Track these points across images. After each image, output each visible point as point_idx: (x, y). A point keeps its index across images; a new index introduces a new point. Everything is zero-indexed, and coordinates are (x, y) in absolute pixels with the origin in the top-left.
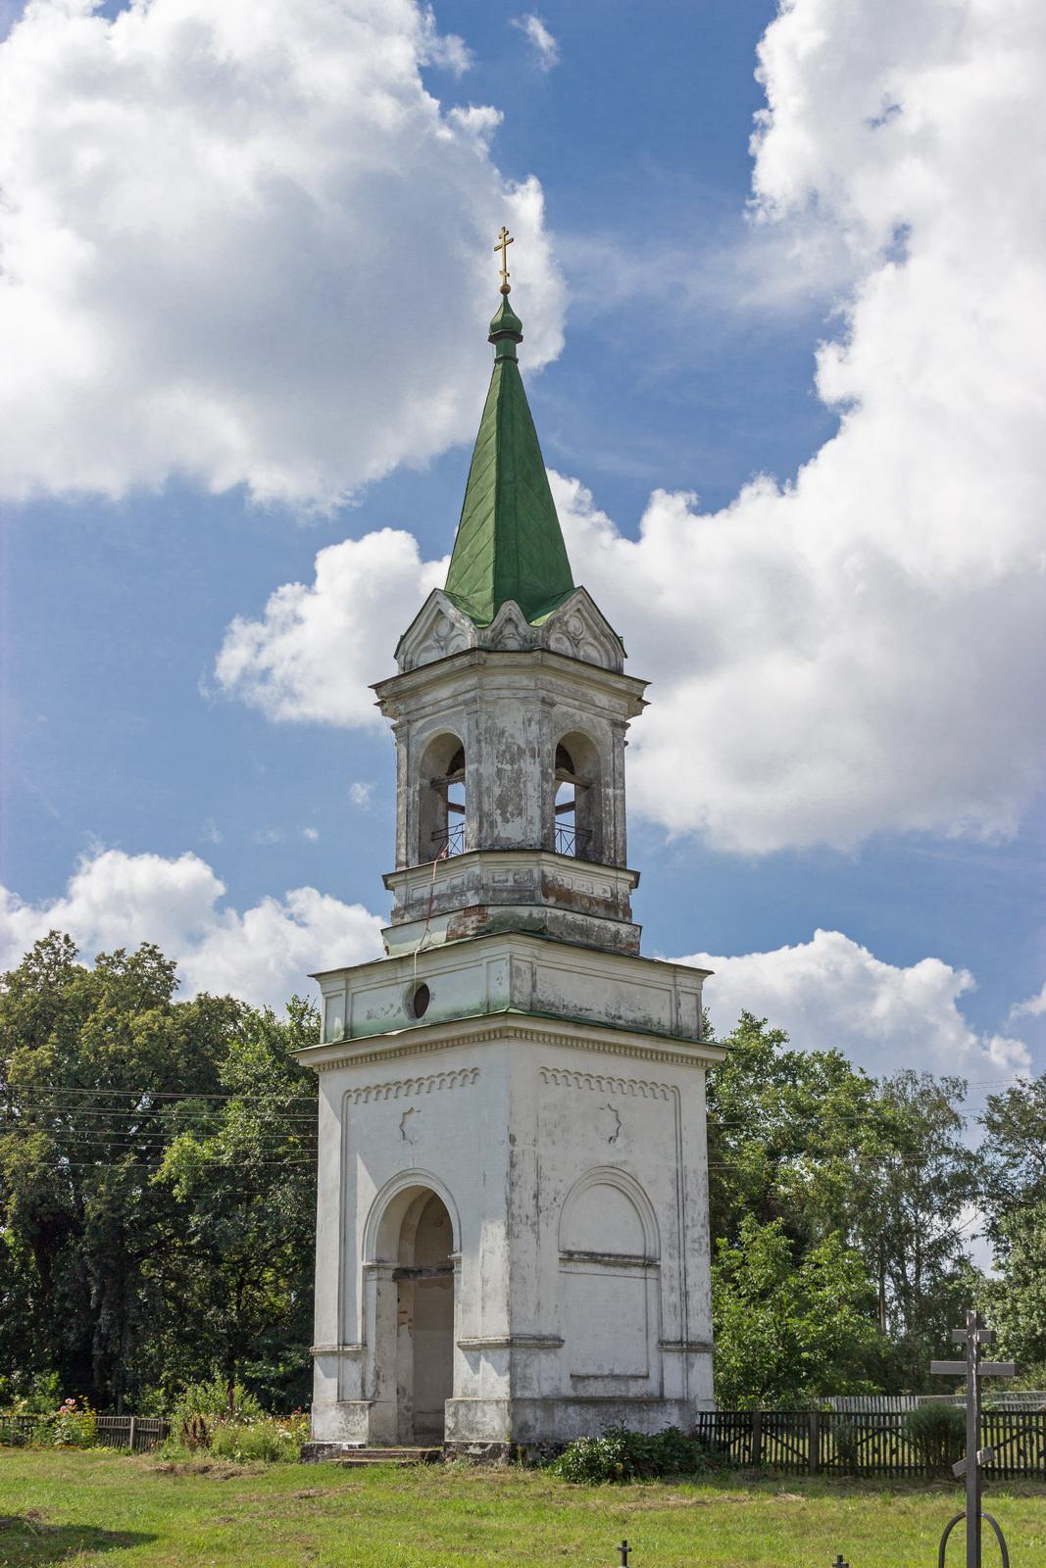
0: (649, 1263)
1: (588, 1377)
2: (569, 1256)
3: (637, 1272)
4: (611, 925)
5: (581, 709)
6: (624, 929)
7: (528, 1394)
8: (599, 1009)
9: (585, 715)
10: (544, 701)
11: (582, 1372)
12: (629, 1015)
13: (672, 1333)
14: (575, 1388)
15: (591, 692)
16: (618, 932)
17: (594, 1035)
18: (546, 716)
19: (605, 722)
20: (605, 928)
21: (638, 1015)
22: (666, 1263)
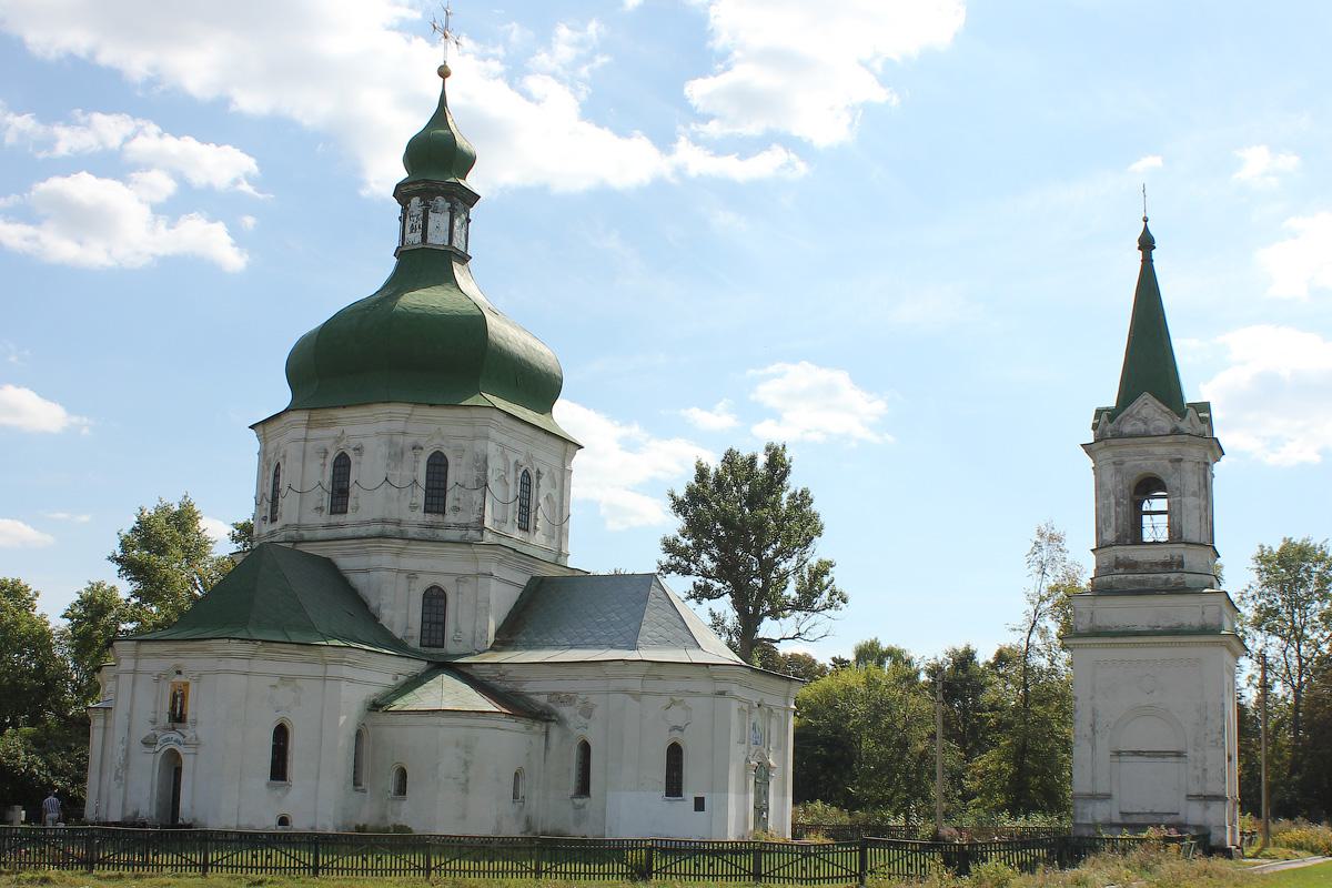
0: (1179, 754)
1: (1132, 814)
2: (1119, 753)
3: (1174, 759)
4: (1164, 576)
5: (1145, 459)
6: (1173, 577)
7: (1085, 822)
8: (1142, 625)
9: (1149, 463)
10: (1114, 463)
11: (1129, 810)
12: (1164, 623)
13: (1195, 791)
14: (1122, 818)
15: (1151, 449)
16: (1168, 579)
17: (1147, 639)
18: (1118, 471)
19: (1166, 462)
20: (1159, 578)
21: (1173, 623)
22: (1190, 753)
